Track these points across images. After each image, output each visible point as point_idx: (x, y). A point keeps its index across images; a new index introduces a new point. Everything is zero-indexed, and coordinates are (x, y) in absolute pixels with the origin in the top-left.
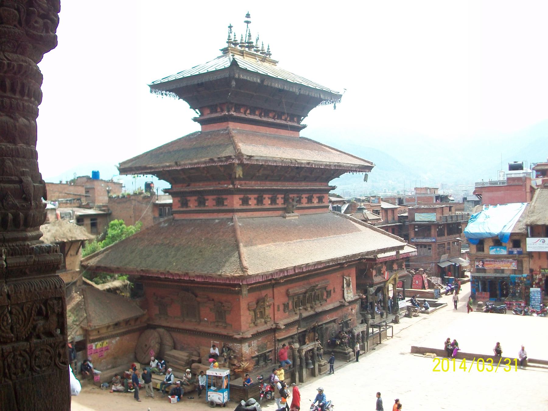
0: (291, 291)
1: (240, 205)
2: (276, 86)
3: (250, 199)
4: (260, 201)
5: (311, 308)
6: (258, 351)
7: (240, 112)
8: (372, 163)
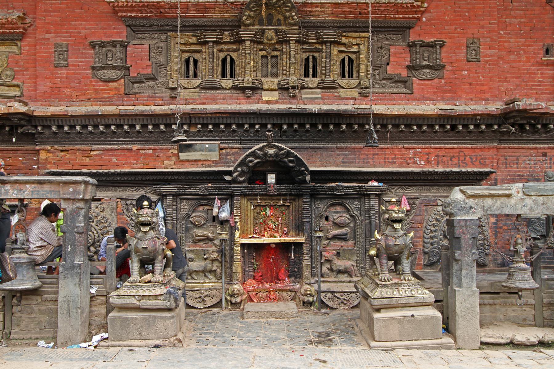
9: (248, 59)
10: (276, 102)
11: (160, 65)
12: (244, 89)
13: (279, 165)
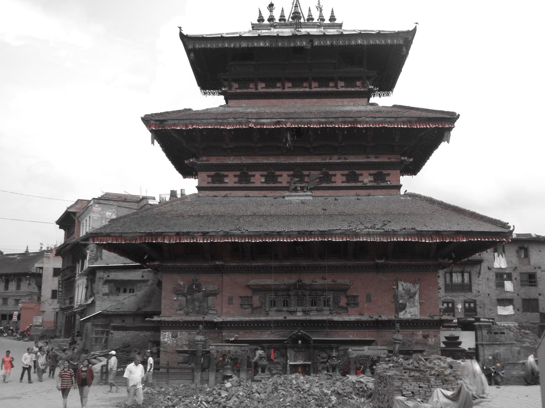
0: (252, 282)
1: (208, 183)
2: (262, 44)
3: (227, 176)
4: (244, 177)
5: (305, 312)
6: (189, 345)
7: (248, 88)
8: (453, 114)
9: (293, 301)
10: (302, 316)
11: (262, 303)
12: (291, 312)
13: (302, 338)
